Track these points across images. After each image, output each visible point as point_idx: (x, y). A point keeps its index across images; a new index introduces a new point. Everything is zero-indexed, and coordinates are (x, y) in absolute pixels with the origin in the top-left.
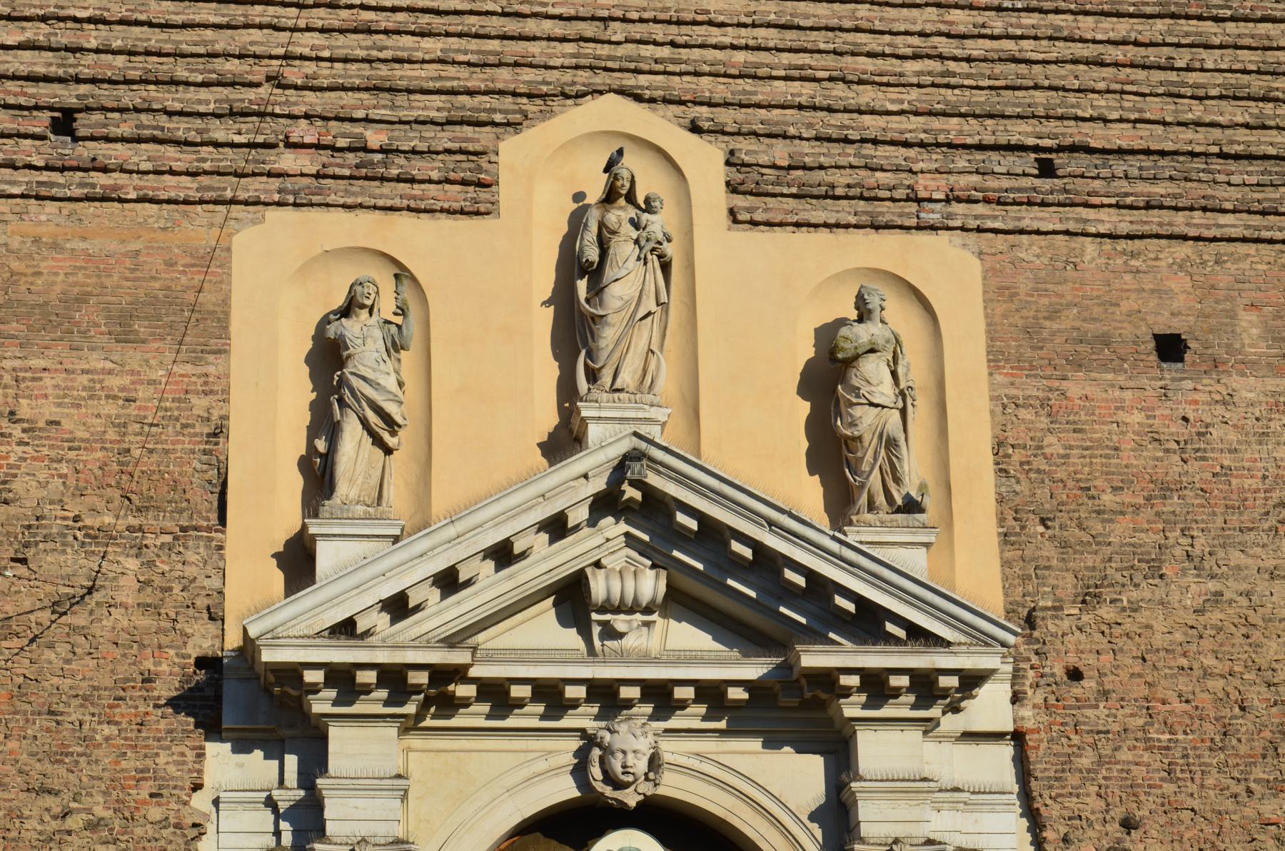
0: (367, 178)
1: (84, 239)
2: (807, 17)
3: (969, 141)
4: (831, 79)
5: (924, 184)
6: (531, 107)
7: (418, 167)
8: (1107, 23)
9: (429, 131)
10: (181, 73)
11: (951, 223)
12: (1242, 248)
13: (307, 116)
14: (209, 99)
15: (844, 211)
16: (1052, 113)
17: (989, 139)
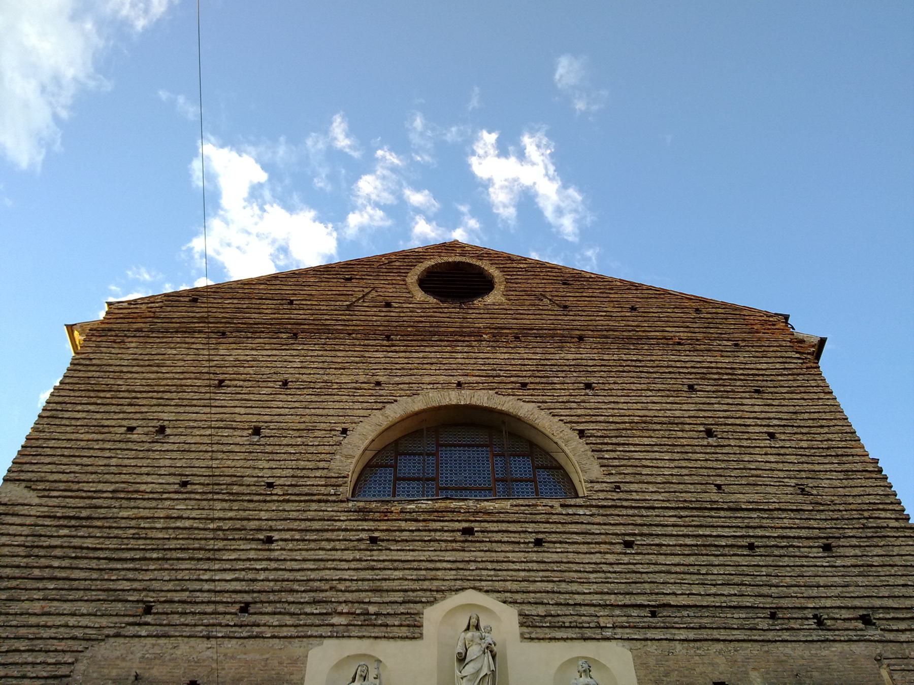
0: (368, 625)
1: (245, 654)
2: (548, 558)
3: (620, 603)
4: (560, 581)
5: (603, 622)
6: (438, 596)
7: (390, 621)
8: (670, 558)
9: (395, 606)
10: (296, 587)
11: (616, 636)
12: (745, 645)
13: (345, 602)
14: (307, 597)
15: (570, 634)
16: (653, 592)
17: (628, 602)
